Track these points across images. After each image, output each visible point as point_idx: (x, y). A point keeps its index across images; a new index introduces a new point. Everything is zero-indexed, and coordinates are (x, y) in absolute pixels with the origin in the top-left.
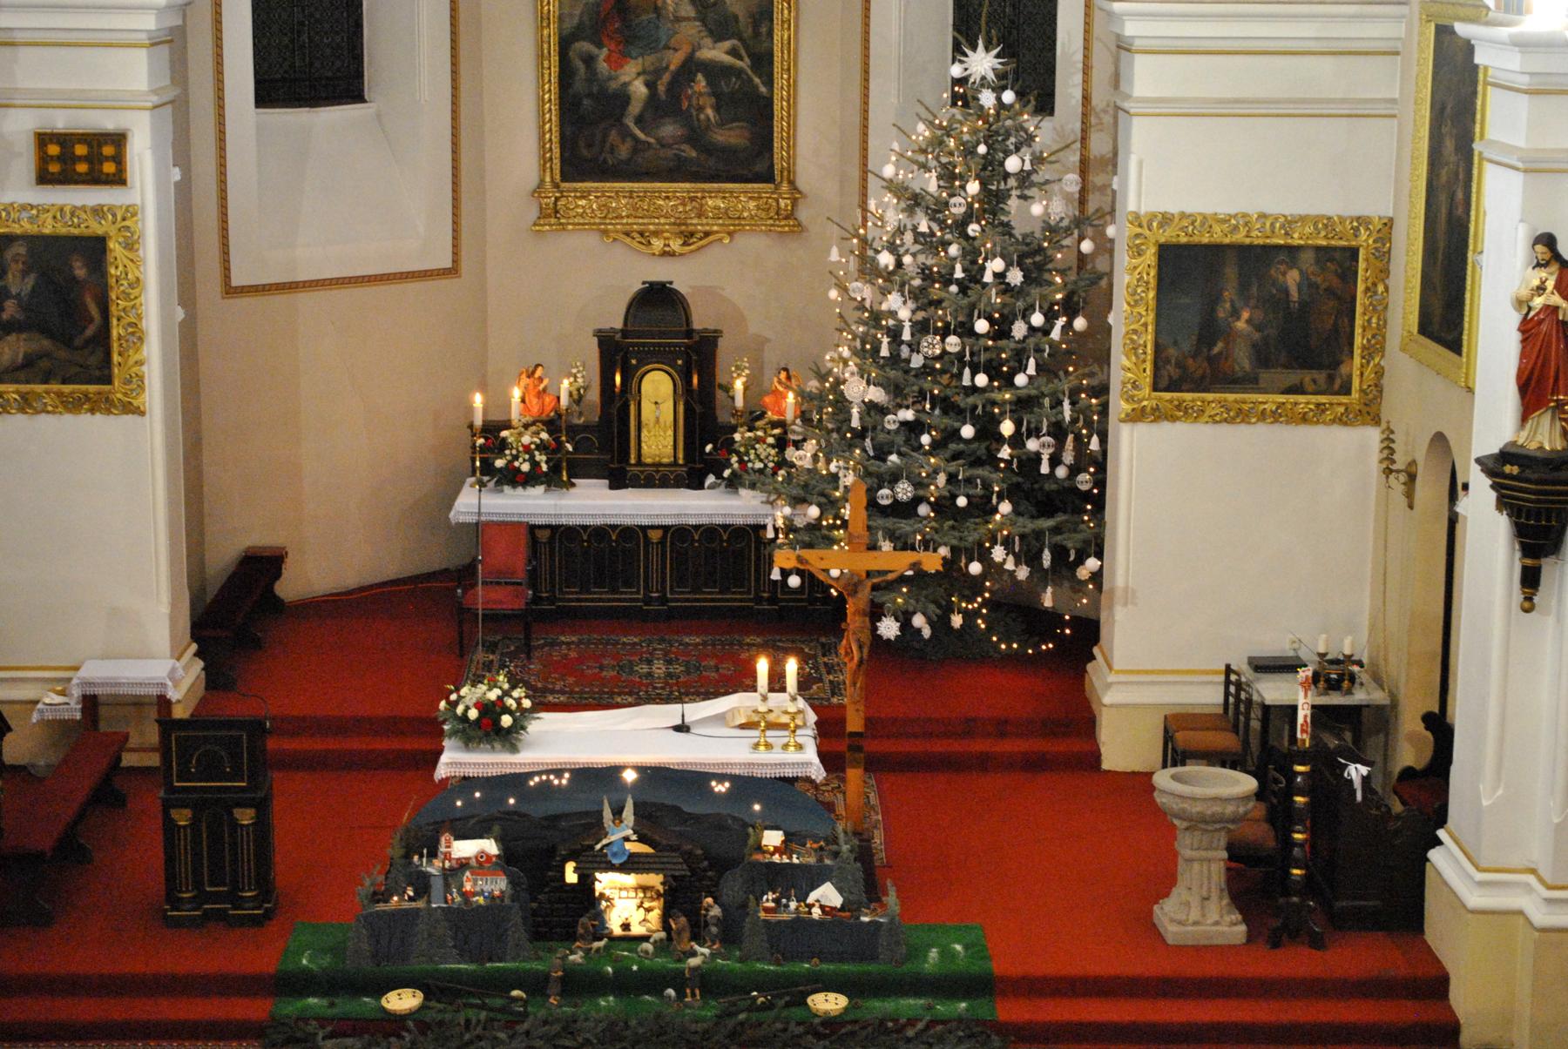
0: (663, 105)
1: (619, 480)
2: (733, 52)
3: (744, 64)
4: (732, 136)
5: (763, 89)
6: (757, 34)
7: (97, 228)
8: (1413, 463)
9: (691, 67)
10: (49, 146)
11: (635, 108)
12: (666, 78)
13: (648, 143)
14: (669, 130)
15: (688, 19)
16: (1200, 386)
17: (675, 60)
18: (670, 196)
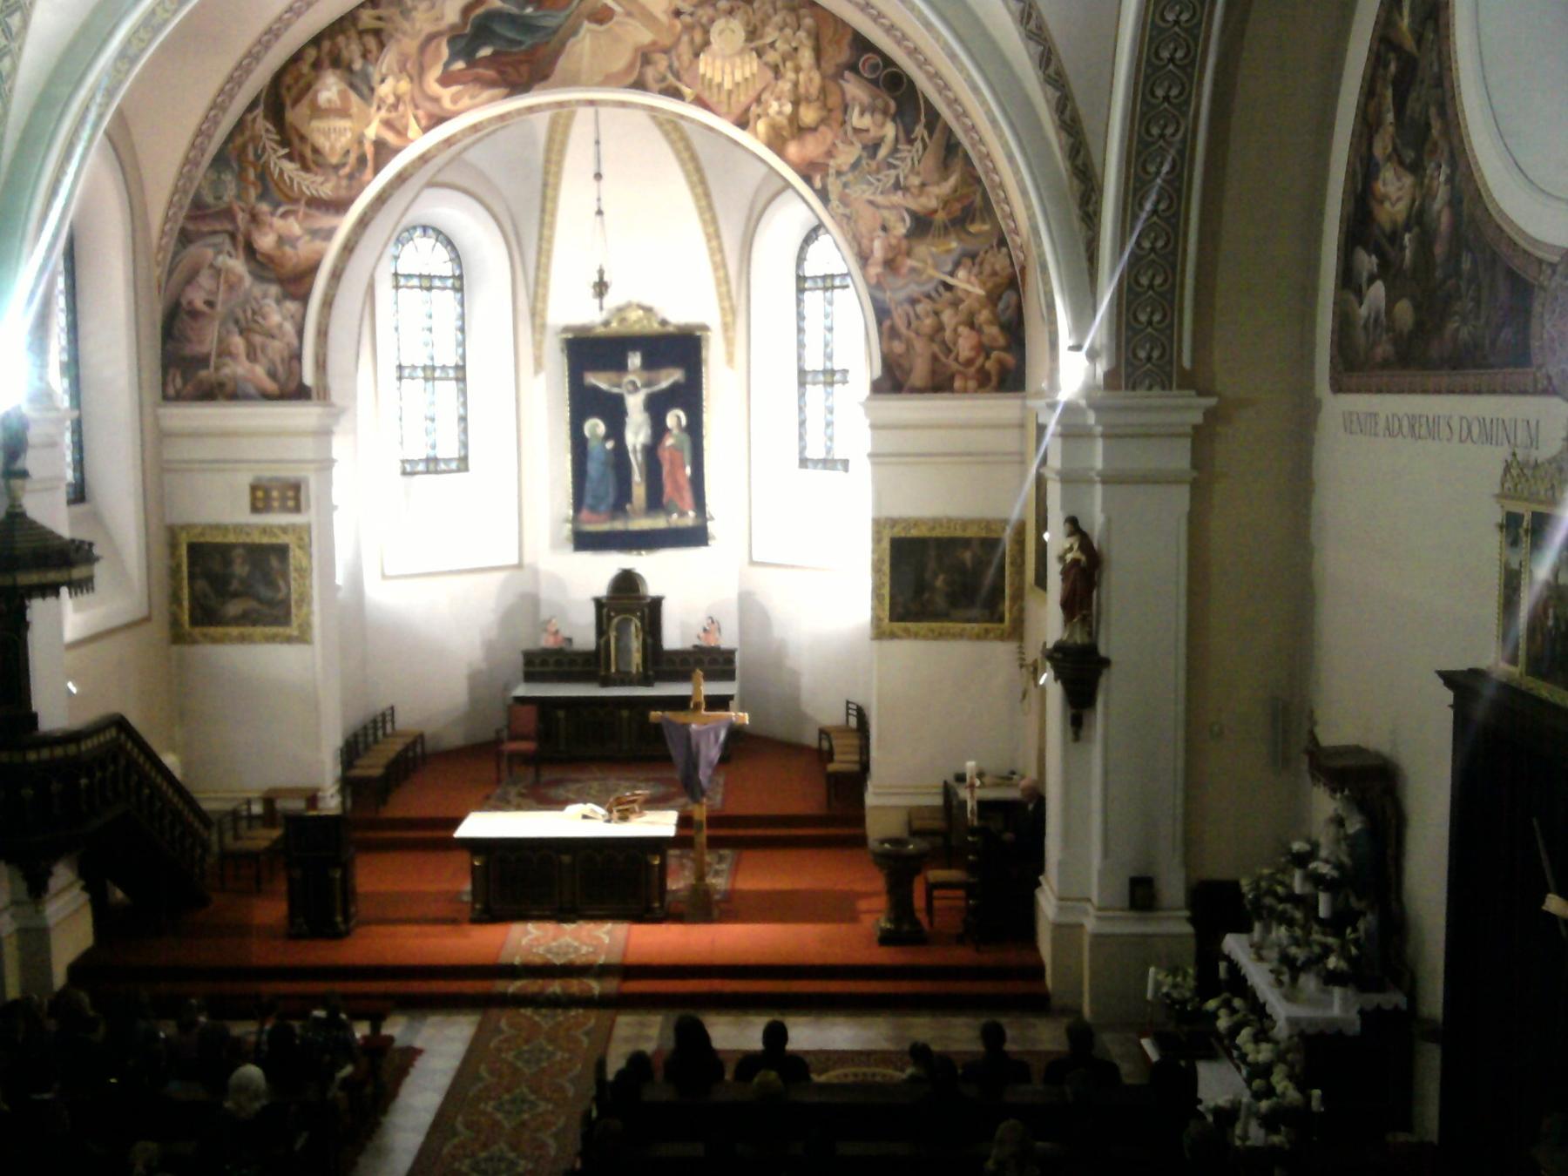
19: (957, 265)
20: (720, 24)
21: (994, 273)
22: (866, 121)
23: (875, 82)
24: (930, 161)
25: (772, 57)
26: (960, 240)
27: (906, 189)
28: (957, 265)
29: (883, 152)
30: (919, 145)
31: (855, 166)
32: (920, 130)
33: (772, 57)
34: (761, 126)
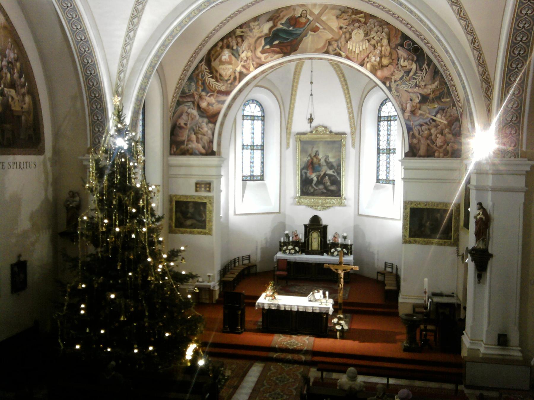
0: (320, 181)
1: (308, 253)
2: (333, 172)
3: (335, 174)
4: (333, 188)
5: (339, 179)
6: (338, 169)
7: (205, 201)
8: (463, 254)
9: (325, 175)
10: (126, 147)
11: (314, 182)
12: (320, 177)
13: (316, 189)
14: (321, 187)
15: (325, 166)
16: (419, 236)
17: (322, 174)
18: (321, 200)
19: (437, 113)
20: (355, 31)
21: (451, 116)
22: (406, 63)
23: (409, 50)
24: (428, 77)
25: (373, 42)
26: (438, 104)
27: (419, 87)
28: (437, 113)
29: (411, 74)
30: (424, 71)
31: (401, 78)
32: (425, 66)
33: (373, 42)
34: (368, 65)
